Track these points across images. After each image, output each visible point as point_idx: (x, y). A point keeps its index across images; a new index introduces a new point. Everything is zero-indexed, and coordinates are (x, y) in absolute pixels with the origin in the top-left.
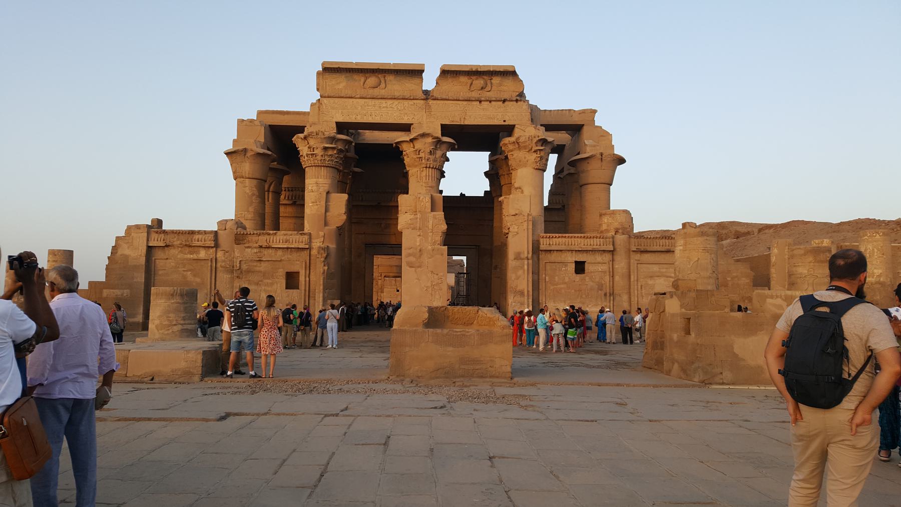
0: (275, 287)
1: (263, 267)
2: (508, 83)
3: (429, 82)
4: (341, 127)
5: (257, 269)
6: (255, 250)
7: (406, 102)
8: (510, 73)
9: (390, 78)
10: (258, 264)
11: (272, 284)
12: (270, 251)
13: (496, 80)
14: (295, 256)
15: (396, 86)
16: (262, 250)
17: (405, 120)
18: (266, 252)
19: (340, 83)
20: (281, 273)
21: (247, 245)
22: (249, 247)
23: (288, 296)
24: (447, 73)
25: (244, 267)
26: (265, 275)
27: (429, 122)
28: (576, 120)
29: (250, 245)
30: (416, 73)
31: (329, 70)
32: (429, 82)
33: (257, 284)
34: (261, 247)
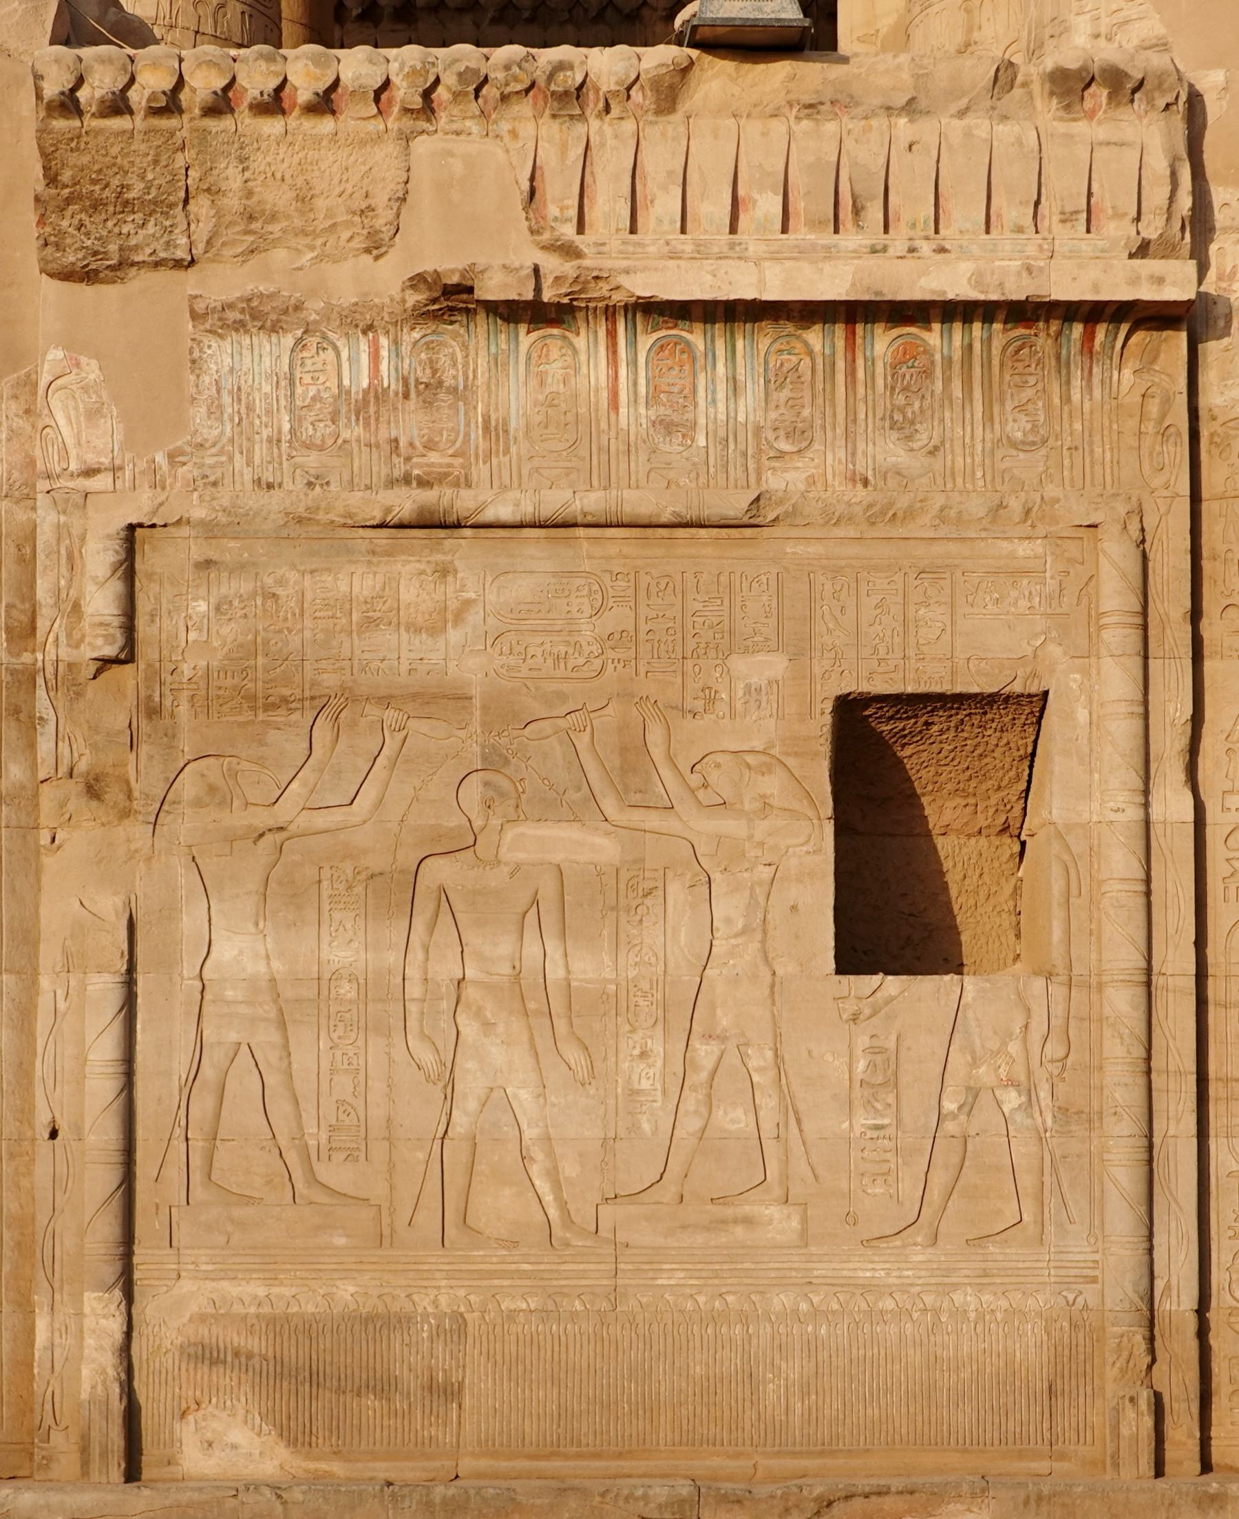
0: (669, 935)
1: (464, 621)
5: (399, 654)
6: (356, 365)
10: (408, 576)
11: (624, 894)
12: (583, 362)
14: (970, 435)
16: (471, 350)
18: (518, 377)
21: (223, 282)
22: (254, 317)
23: (886, 1076)
25: (194, 624)
26: (505, 744)
29: (279, 270)
33: (398, 891)
34: (451, 300)
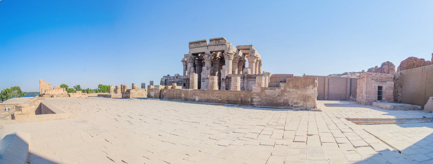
2: (223, 41)
3: (208, 43)
4: (193, 54)
7: (203, 48)
8: (222, 39)
9: (201, 43)
13: (221, 40)
15: (202, 44)
17: (203, 51)
19: (192, 45)
20: (183, 83)
24: (211, 40)
27: (207, 51)
28: (248, 48)
30: (205, 41)
31: (190, 43)
32: (208, 43)
